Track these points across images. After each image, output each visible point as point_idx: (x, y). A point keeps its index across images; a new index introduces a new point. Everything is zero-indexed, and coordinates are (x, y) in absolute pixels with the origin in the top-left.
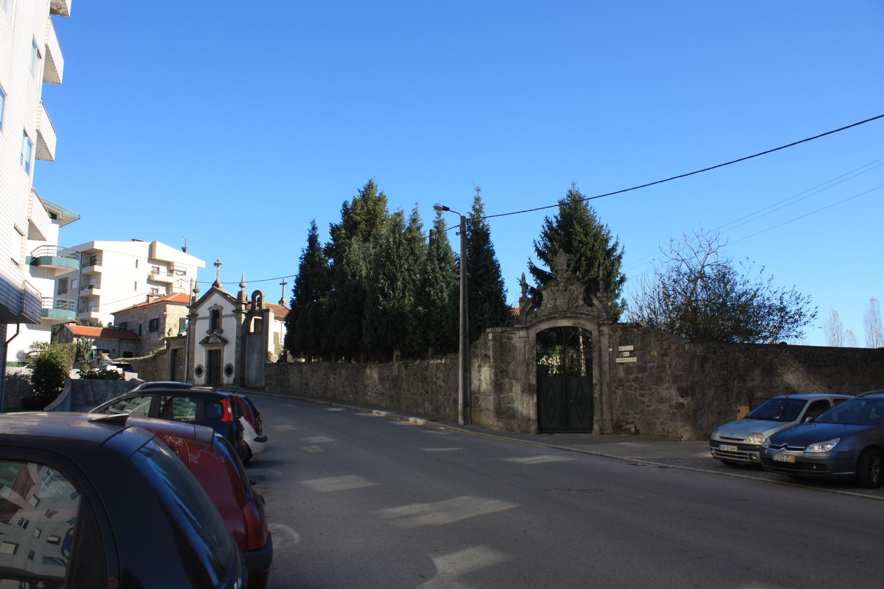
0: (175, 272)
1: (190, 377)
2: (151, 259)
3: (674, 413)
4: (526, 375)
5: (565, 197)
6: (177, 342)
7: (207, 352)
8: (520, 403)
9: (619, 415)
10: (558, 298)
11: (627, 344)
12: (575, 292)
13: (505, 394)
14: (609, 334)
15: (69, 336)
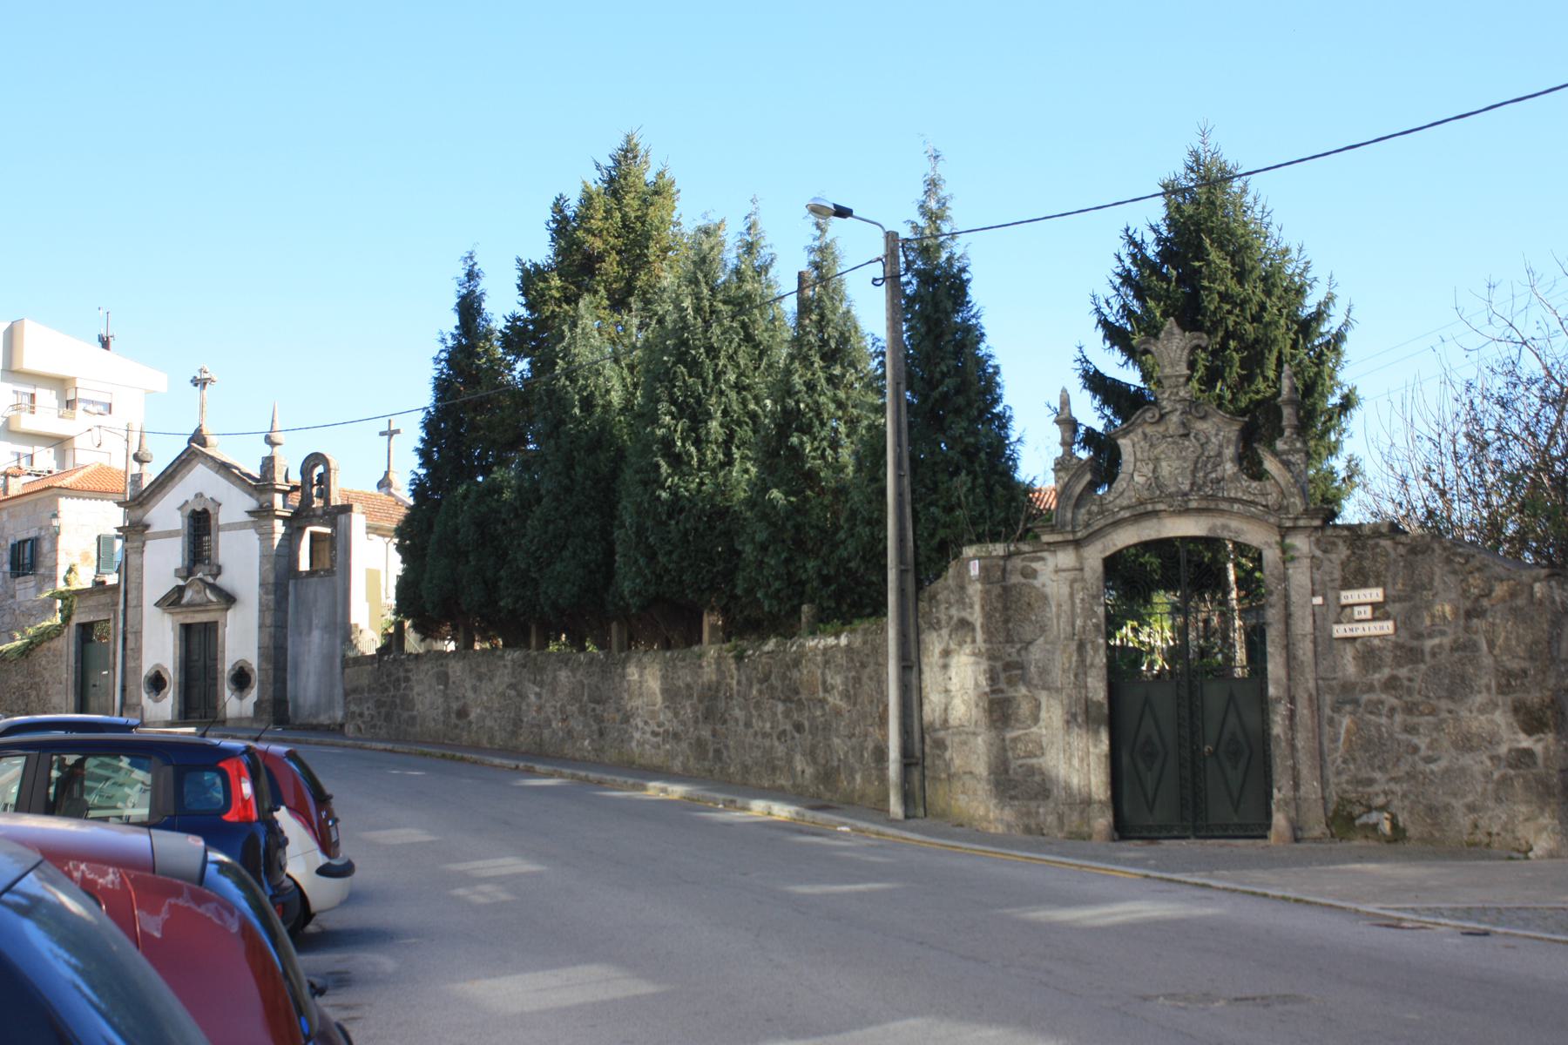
0: (80, 406)
1: (132, 700)
3: (1504, 780)
4: (1076, 676)
5: (1181, 170)
6: (92, 602)
7: (178, 627)
8: (1061, 756)
9: (1345, 786)
10: (1163, 456)
11: (1365, 585)
12: (1213, 440)
13: (1019, 729)
14: (1313, 557)
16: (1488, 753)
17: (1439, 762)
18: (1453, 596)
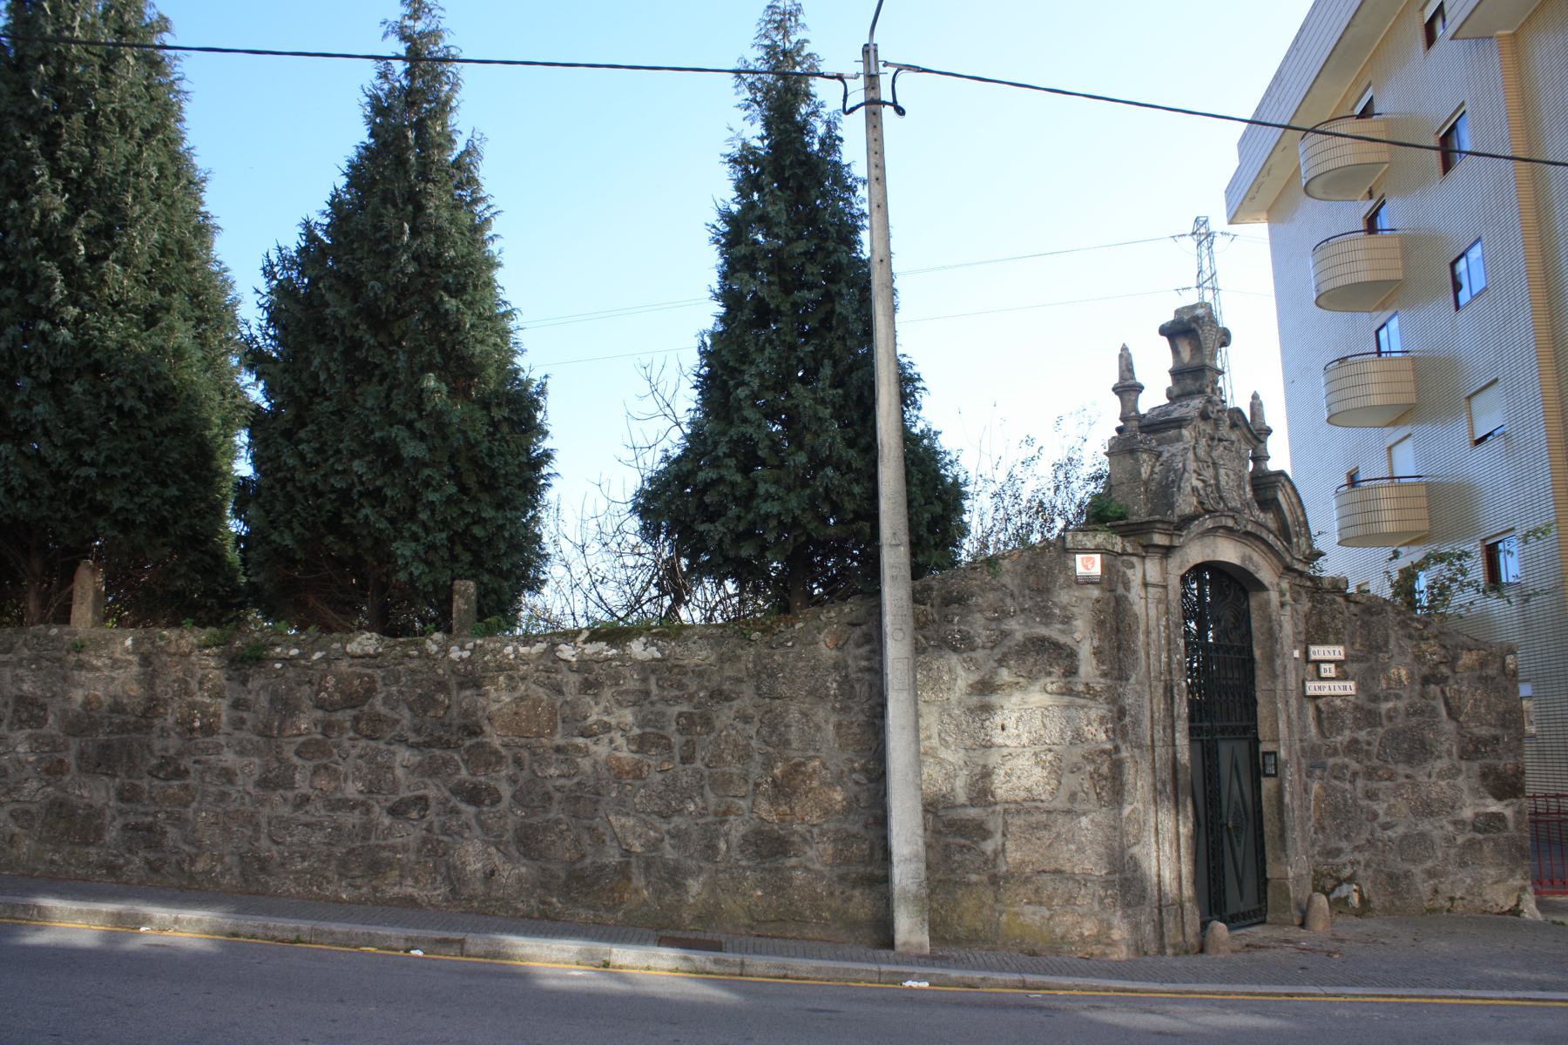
3: (1471, 844)
16: (1450, 818)
17: (1396, 829)
18: (1408, 660)
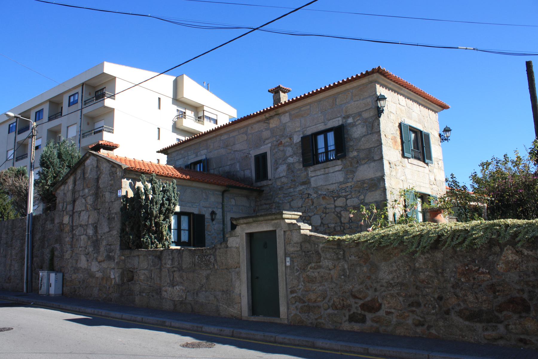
2: (177, 100)
15: (105, 179)
